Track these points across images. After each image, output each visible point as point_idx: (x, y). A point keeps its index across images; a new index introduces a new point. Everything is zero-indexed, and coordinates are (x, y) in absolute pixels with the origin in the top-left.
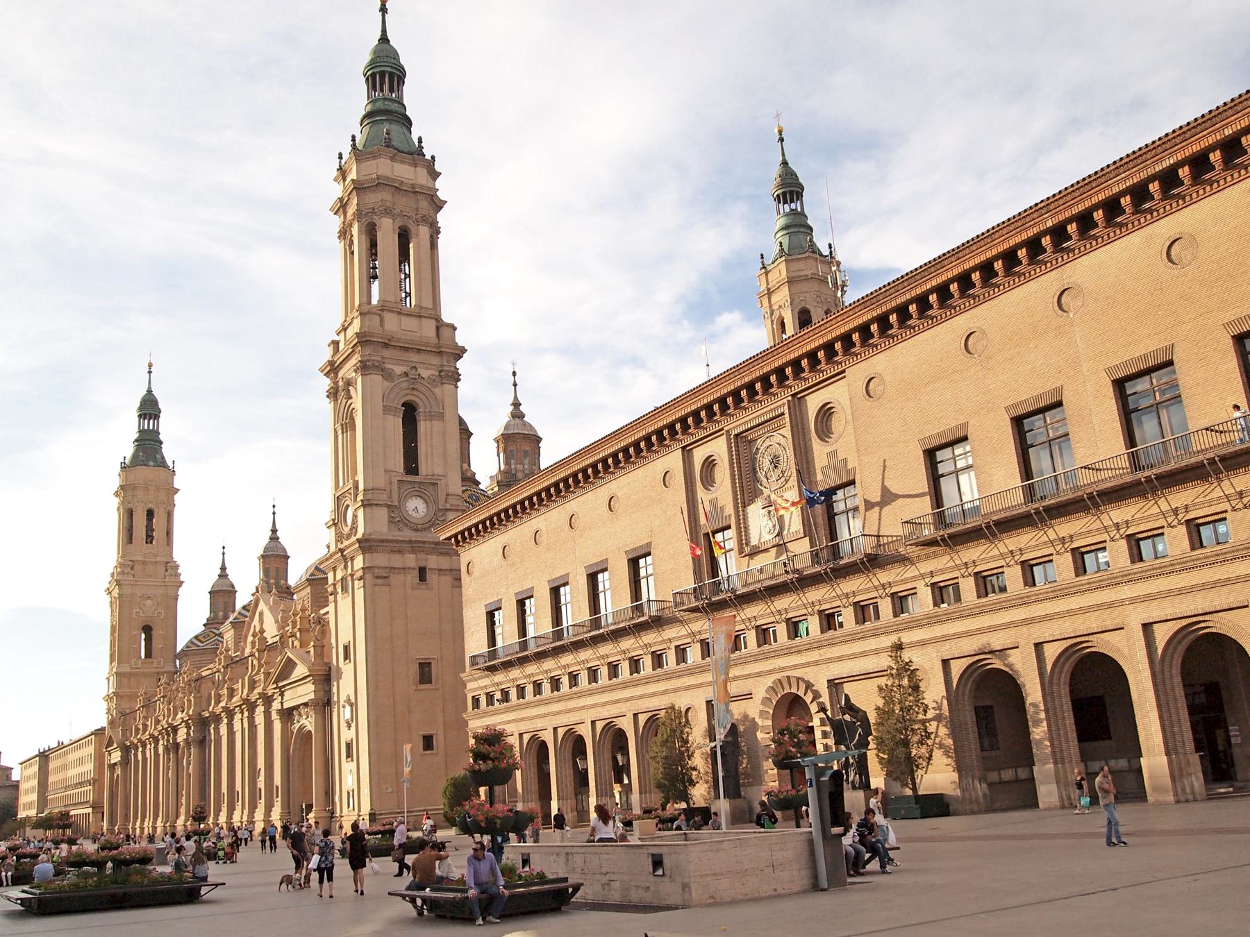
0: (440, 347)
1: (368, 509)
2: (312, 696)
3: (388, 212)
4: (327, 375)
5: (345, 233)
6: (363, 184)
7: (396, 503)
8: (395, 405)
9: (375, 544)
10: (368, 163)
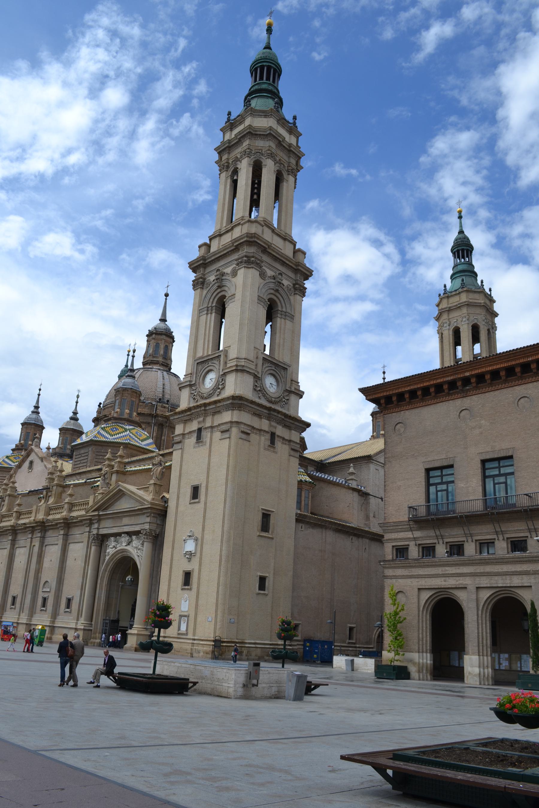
0: (299, 265)
1: (239, 374)
2: (147, 527)
3: (272, 156)
4: (194, 270)
5: (228, 167)
6: (256, 131)
7: (260, 376)
8: (265, 297)
9: (246, 403)
10: (261, 119)
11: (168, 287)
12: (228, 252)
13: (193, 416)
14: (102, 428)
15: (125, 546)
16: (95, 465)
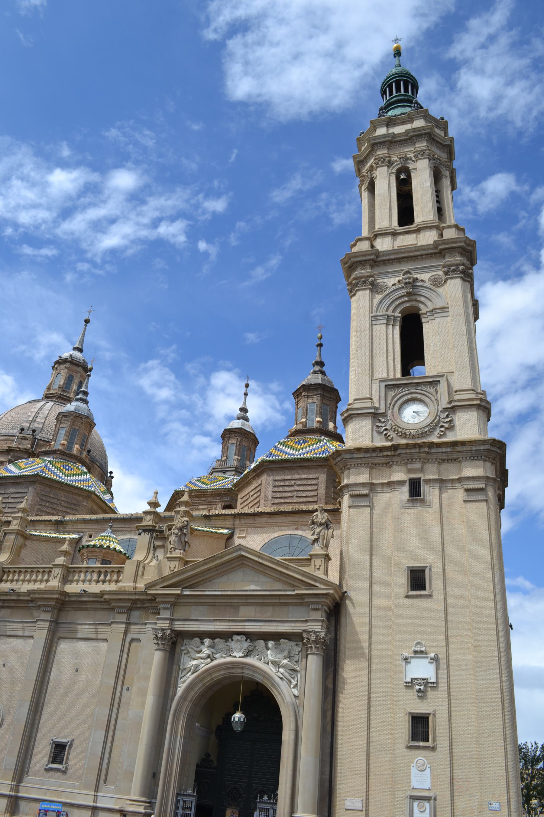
6: (435, 136)
11: (90, 312)
12: (421, 255)
13: (395, 459)
14: (50, 461)
15: (240, 657)
16: (37, 515)
